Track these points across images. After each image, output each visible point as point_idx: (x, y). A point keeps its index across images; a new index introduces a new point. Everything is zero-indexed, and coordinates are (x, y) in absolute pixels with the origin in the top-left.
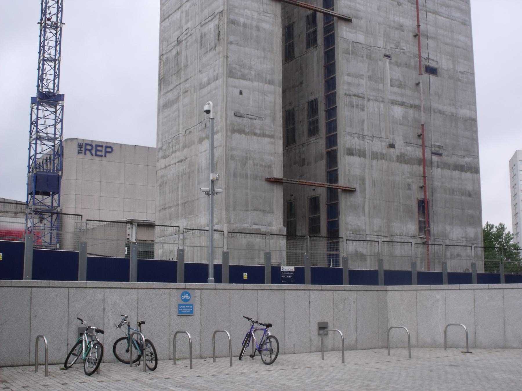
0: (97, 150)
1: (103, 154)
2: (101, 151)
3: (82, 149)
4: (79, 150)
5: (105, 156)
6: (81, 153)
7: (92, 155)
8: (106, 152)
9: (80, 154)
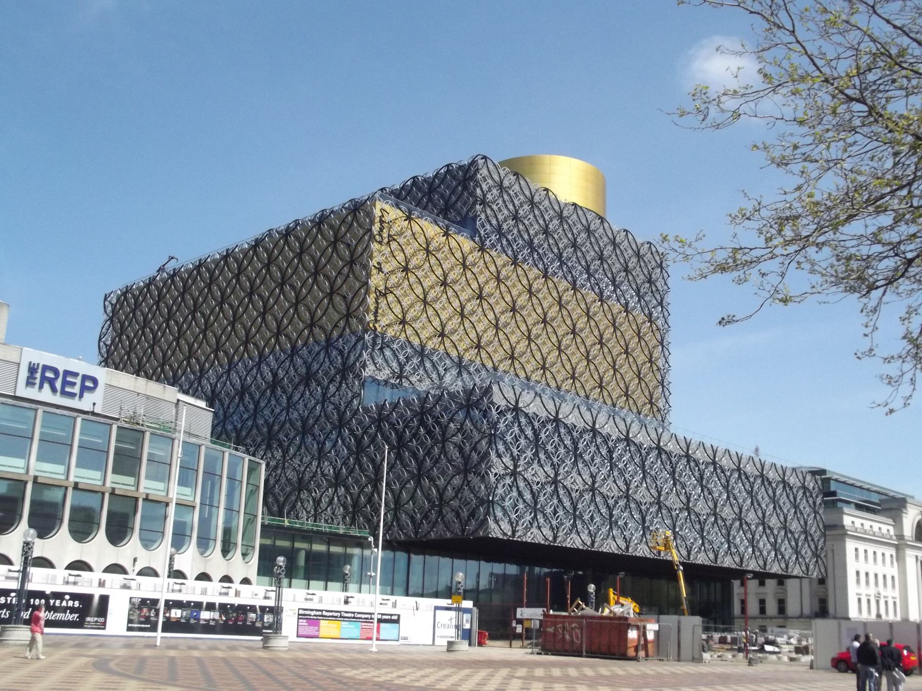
0: (65, 383)
1: (76, 390)
2: (73, 384)
5: (81, 396)
7: (54, 390)
8: (84, 389)
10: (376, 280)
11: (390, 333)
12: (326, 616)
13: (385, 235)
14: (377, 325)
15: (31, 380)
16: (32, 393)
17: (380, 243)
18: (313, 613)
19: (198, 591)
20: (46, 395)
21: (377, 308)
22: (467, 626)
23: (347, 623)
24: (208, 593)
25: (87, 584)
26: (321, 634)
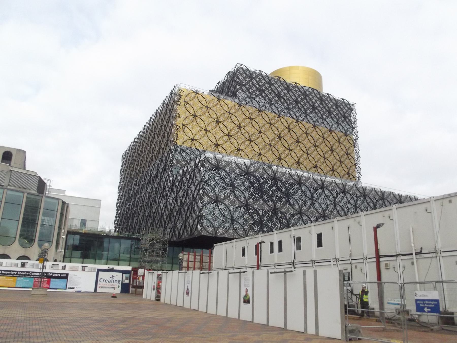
10: (179, 122)
11: (185, 145)
12: (5, 274)
13: (182, 101)
14: (177, 142)
17: (179, 105)
21: (177, 134)
22: (127, 281)
23: (22, 278)
24: (3, 265)
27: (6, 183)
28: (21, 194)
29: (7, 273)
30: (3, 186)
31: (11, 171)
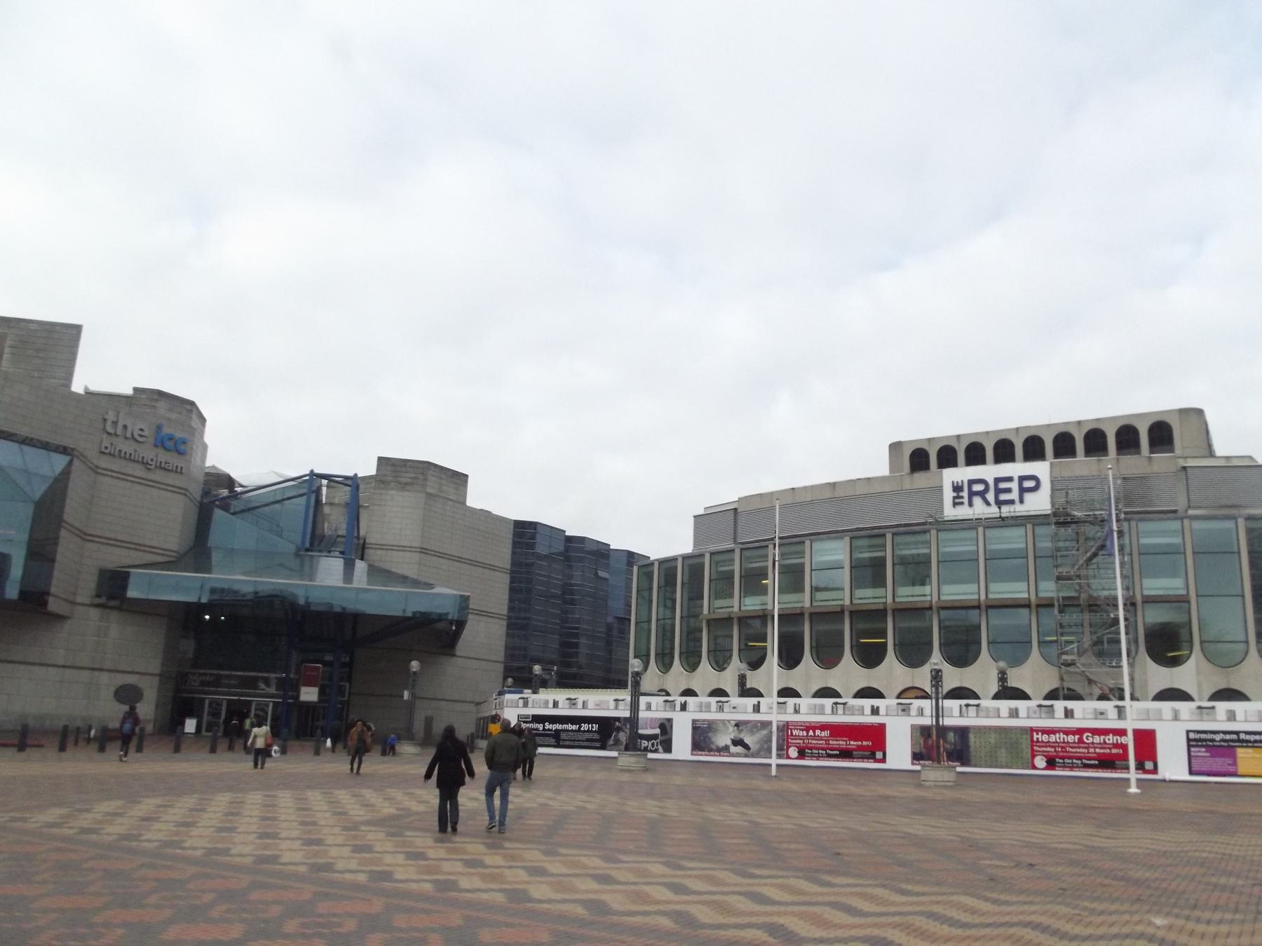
0: (998, 491)
1: (1014, 495)
2: (1009, 490)
3: (961, 494)
4: (954, 498)
5: (1022, 501)
6: (962, 503)
7: (988, 504)
8: (1023, 491)
9: (957, 507)
15: (957, 501)
16: (964, 512)
18: (1218, 737)
19: (1004, 712)
20: (980, 509)
25: (860, 713)
26: (1241, 770)
27: (1181, 504)
28: (1229, 524)
29: (1252, 738)
30: (1175, 512)
31: (1184, 468)
